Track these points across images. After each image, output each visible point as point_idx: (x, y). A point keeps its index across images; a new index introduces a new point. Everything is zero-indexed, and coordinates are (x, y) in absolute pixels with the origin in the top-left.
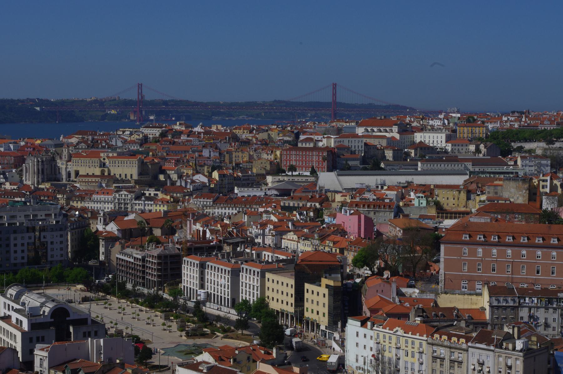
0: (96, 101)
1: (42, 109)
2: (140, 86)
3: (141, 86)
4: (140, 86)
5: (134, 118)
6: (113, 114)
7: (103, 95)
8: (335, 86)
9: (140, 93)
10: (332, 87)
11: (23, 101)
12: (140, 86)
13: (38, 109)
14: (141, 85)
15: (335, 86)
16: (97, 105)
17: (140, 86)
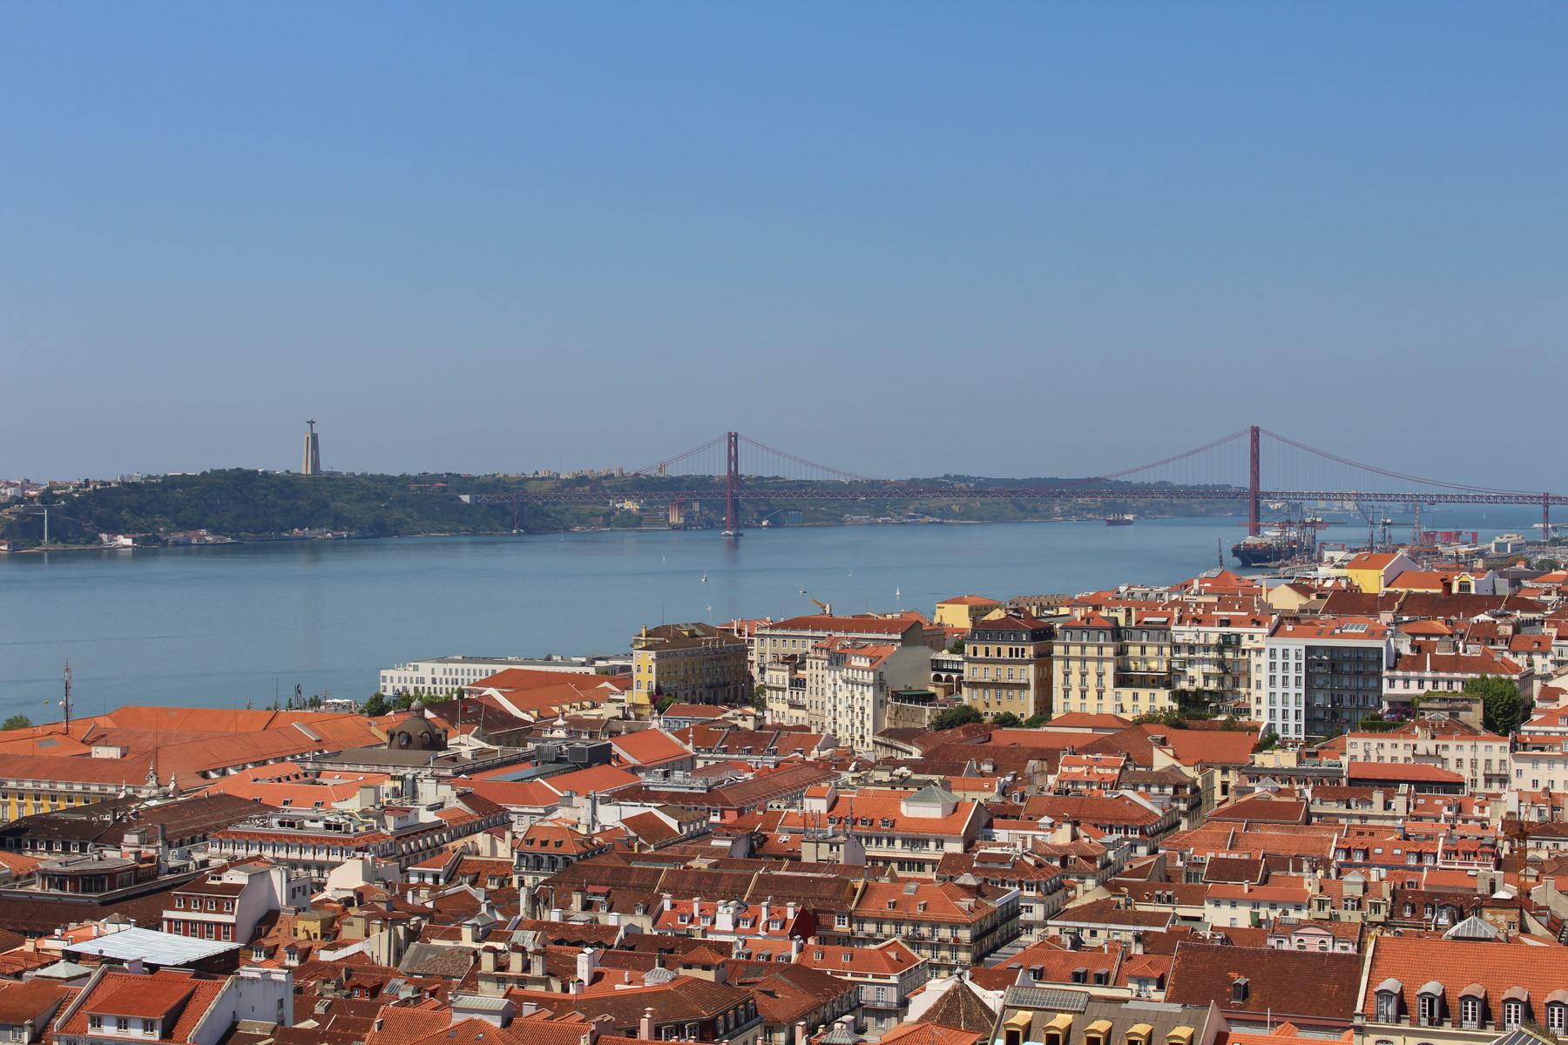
0: (581, 480)
1: (474, 499)
2: (733, 439)
3: (736, 440)
4: (733, 439)
5: (679, 520)
6: (629, 511)
7: (598, 463)
8: (1255, 432)
9: (733, 459)
10: (1249, 435)
11: (416, 480)
13: (466, 498)
14: (736, 436)
15: (1255, 432)
16: (588, 488)
17: (733, 439)
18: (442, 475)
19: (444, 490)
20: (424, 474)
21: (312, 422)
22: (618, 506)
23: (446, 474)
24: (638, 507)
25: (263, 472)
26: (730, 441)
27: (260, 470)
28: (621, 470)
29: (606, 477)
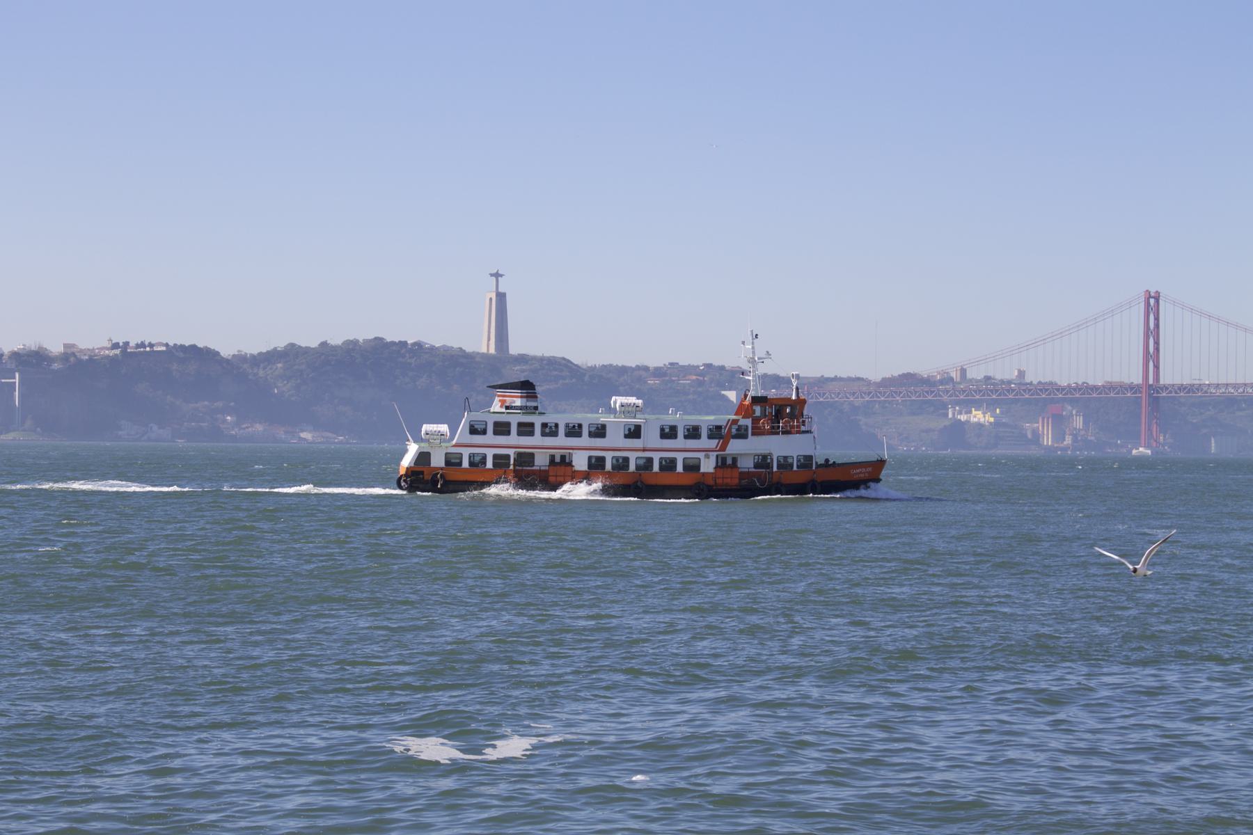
2: (1152, 302)
4: (1152, 301)
11: (658, 372)
12: (1152, 301)
17: (1152, 302)
18: (698, 367)
19: (701, 383)
20: (671, 364)
21: (497, 275)
22: (963, 418)
23: (704, 365)
24: (992, 420)
25: (415, 344)
26: (1148, 304)
27: (409, 342)
28: (963, 372)
29: (942, 382)
